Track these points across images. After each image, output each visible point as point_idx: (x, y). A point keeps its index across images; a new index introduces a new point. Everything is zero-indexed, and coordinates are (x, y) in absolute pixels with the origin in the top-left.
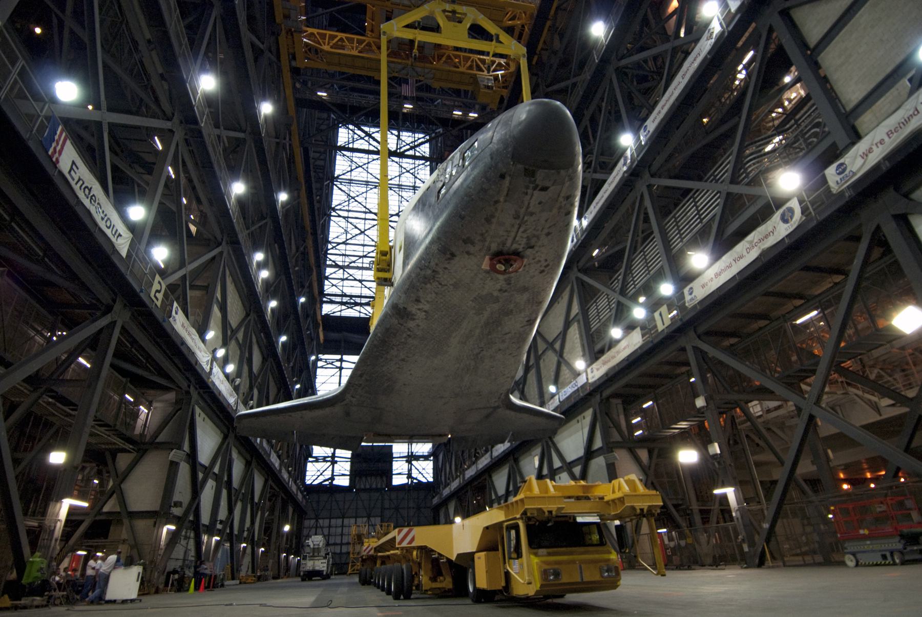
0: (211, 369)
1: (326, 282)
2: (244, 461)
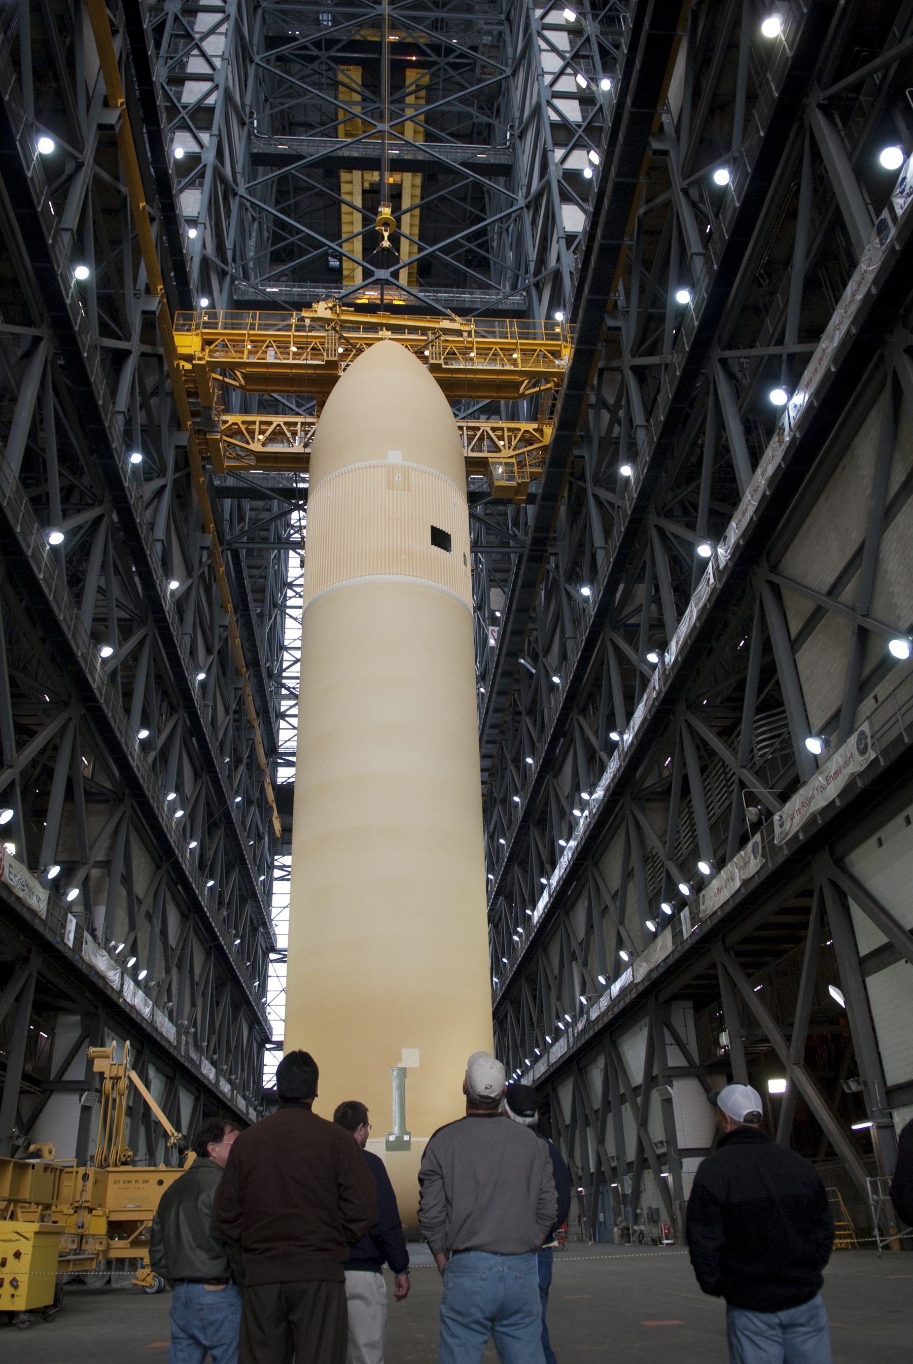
0: (122, 985)
1: (283, 724)
2: (164, 1079)
